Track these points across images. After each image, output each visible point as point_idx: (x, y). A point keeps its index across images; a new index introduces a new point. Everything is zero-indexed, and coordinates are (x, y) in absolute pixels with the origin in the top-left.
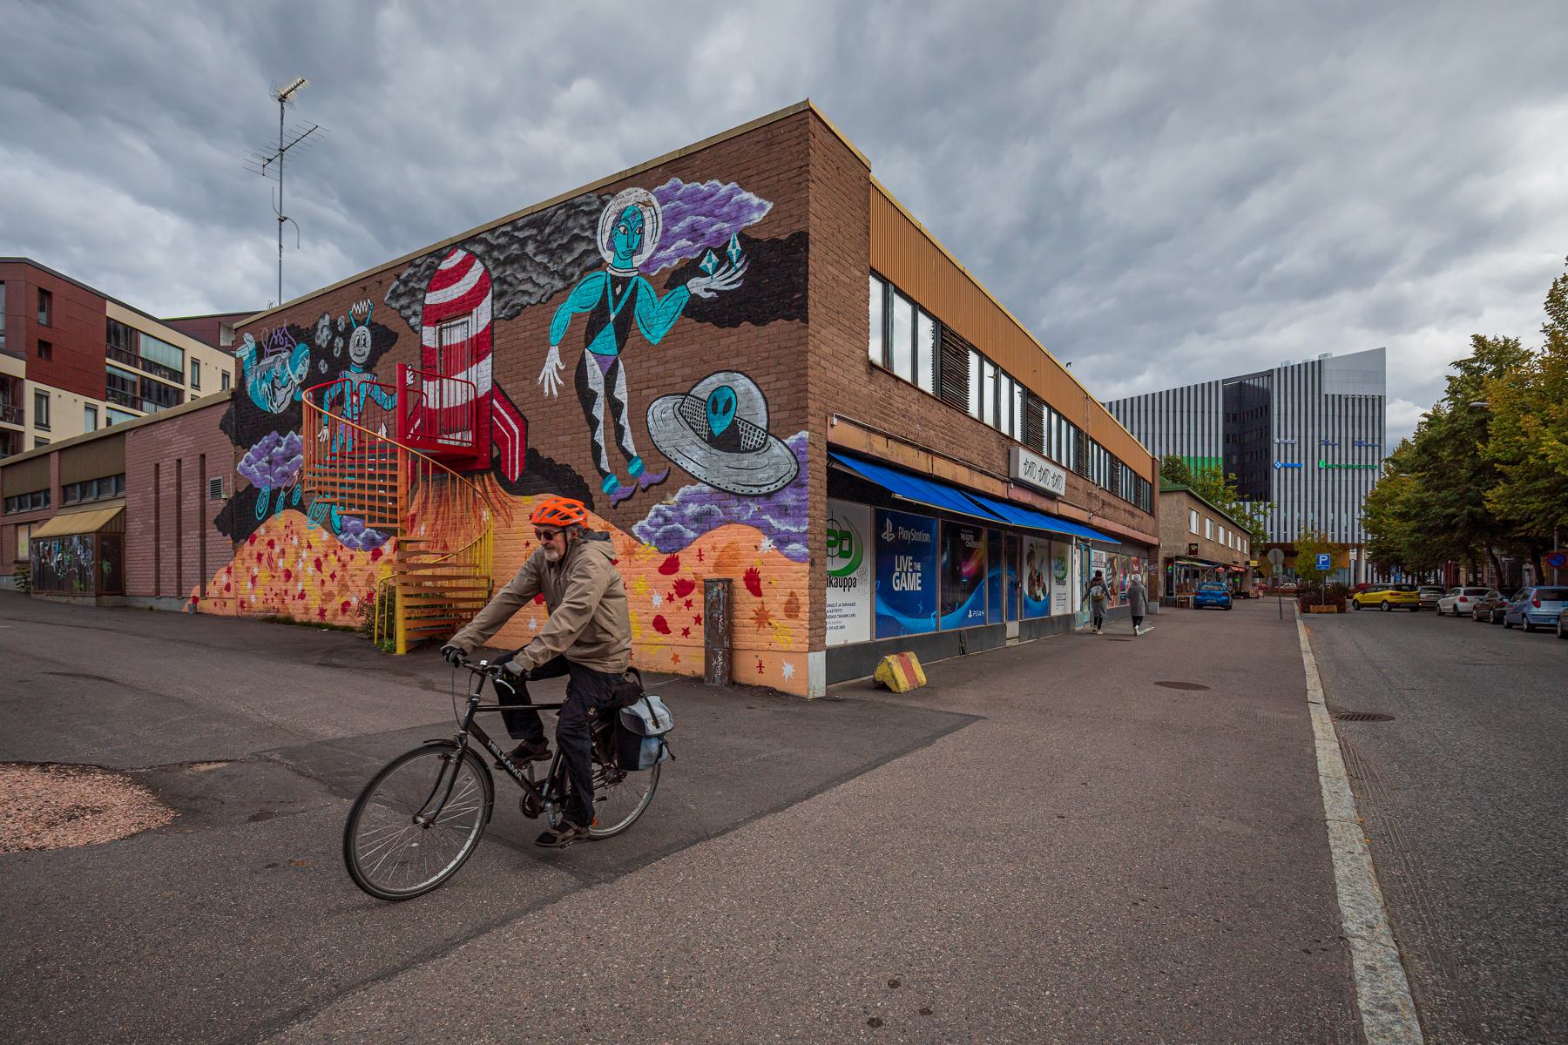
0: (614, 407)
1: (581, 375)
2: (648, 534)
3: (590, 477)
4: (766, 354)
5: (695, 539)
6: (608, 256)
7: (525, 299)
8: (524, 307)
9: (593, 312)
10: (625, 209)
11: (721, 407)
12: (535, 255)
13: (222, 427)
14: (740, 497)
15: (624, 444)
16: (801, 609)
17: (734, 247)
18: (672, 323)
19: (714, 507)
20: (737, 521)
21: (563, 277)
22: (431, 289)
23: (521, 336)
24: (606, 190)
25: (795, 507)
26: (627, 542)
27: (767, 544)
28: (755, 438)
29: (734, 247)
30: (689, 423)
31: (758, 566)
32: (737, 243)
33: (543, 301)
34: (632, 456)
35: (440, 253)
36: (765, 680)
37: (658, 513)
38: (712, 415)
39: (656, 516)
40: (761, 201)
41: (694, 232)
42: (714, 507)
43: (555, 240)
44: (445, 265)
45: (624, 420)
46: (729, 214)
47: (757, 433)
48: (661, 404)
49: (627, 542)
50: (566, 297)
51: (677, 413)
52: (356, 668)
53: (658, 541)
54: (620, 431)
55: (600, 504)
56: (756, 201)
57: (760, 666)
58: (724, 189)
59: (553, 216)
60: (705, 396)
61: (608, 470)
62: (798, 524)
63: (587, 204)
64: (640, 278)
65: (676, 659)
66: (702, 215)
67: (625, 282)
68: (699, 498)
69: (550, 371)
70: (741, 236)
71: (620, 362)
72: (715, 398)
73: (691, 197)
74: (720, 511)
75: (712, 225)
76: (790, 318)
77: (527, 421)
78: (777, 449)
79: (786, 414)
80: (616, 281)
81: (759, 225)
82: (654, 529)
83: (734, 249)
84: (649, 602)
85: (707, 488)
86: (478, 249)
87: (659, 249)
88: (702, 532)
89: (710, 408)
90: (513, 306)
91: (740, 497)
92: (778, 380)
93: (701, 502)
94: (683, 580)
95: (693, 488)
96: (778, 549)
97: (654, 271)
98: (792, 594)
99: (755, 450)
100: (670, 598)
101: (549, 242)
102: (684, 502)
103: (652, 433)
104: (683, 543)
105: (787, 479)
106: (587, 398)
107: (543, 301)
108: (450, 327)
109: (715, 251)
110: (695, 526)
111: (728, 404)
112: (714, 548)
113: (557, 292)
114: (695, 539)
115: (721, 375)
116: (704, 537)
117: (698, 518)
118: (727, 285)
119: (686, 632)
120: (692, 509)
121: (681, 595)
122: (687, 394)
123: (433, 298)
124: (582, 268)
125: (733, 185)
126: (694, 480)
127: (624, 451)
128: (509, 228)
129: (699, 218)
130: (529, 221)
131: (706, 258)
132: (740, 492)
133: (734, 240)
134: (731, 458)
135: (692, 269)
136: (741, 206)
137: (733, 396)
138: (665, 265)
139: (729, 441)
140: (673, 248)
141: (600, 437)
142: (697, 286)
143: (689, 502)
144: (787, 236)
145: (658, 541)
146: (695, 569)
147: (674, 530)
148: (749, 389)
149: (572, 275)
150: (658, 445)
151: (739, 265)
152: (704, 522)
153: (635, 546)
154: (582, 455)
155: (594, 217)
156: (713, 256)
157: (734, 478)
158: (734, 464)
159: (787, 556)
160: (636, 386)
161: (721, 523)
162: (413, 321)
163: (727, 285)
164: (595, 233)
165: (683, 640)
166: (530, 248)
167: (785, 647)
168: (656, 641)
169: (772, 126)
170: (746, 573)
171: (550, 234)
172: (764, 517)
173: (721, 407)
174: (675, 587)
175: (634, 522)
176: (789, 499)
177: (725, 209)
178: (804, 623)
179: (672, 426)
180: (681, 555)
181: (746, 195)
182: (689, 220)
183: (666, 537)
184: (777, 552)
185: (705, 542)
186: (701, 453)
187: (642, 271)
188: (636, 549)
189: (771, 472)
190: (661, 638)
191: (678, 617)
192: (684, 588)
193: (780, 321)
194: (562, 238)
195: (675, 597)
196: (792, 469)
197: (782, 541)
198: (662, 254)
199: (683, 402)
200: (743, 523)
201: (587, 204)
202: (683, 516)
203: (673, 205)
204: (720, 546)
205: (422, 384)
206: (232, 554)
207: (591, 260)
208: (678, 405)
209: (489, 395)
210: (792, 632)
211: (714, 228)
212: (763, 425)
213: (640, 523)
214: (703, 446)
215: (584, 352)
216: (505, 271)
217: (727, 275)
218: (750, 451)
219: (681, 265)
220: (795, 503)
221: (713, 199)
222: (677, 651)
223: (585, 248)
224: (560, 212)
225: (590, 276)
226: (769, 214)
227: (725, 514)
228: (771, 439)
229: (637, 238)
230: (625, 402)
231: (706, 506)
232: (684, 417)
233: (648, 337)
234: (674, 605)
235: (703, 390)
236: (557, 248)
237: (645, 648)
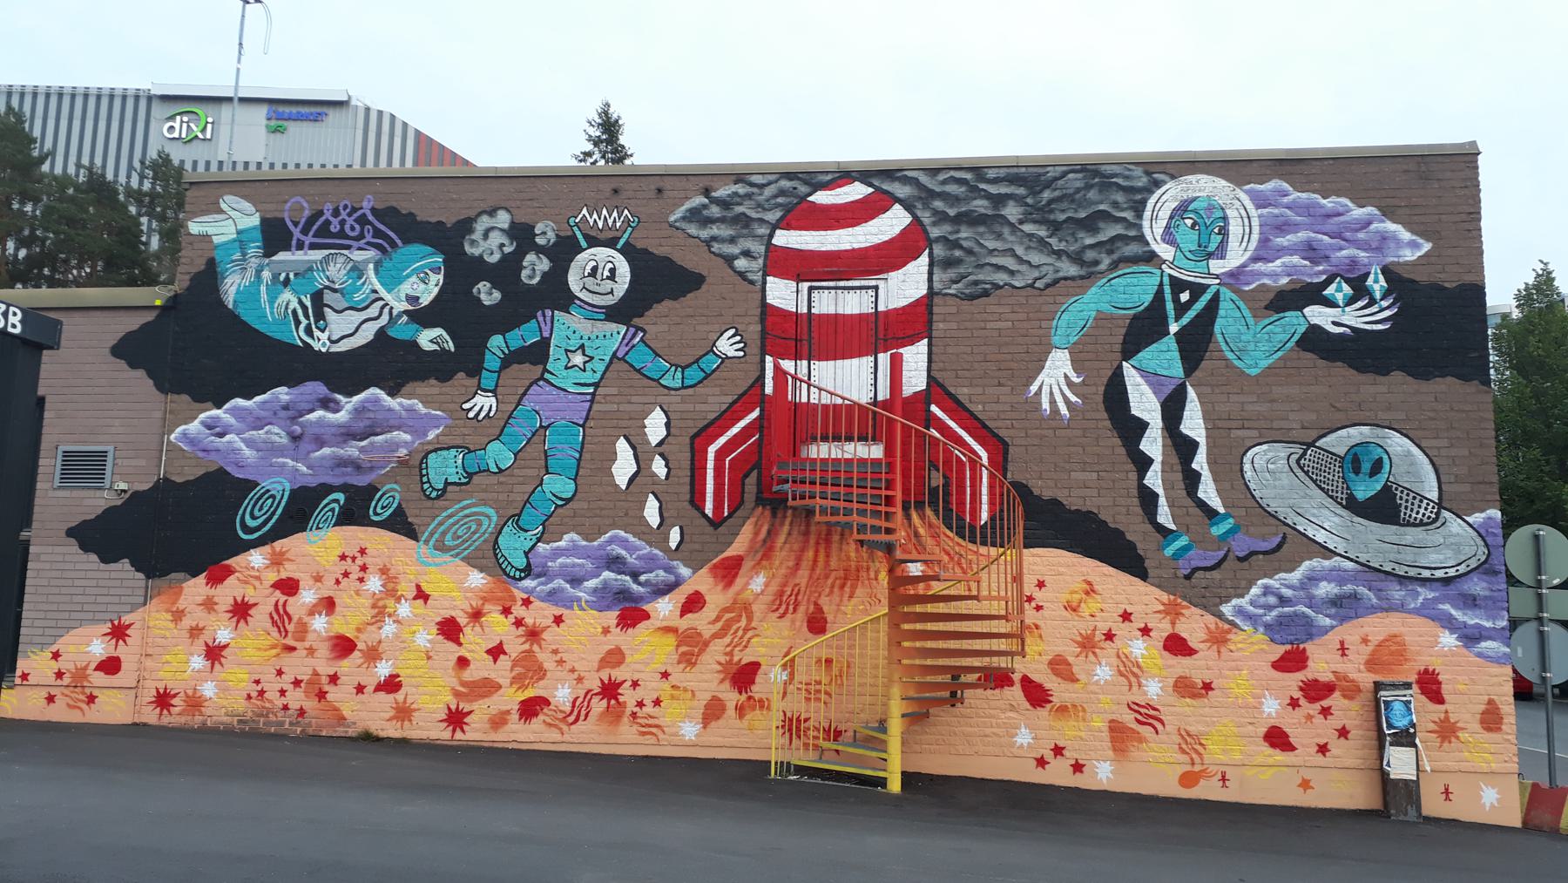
0: (1182, 448)
1: (1116, 395)
2: (1249, 617)
3: (1136, 530)
4: (1432, 414)
5: (1333, 627)
6: (1165, 251)
7: (1001, 278)
8: (997, 287)
9: (1135, 318)
10: (1194, 199)
11: (1366, 467)
12: (1021, 222)
13: (1475, 142)
14: (1403, 580)
15: (1201, 494)
16: (1505, 721)
17: (1376, 281)
18: (1280, 354)
19: (1362, 590)
20: (1401, 608)
21: (1077, 258)
22: (786, 224)
23: (991, 325)
24: (1160, 168)
25: (1486, 598)
26: (1212, 627)
27: (1449, 640)
28: (1422, 511)
29: (1376, 281)
30: (1315, 482)
31: (1436, 664)
32: (1381, 277)
33: (1037, 285)
34: (1215, 513)
35: (814, 178)
36: (1457, 810)
37: (1267, 591)
38: (1352, 475)
39: (1265, 594)
40: (1414, 238)
41: (1311, 252)
42: (1362, 590)
43: (1063, 211)
44: (822, 198)
45: (1200, 462)
46: (1366, 242)
47: (1424, 505)
48: (1269, 450)
49: (1212, 627)
50: (1084, 290)
51: (1294, 466)
52: (1345, 571)
53: (1268, 627)
54: (1192, 479)
55: (1157, 572)
56: (1406, 235)
57: (1447, 792)
58: (1358, 212)
59: (1056, 179)
60: (1341, 451)
61: (1173, 527)
62: (1494, 618)
63: (1127, 178)
64: (1223, 290)
65: (1305, 785)
66: (1324, 234)
67: (1197, 290)
68: (1339, 577)
69: (1053, 381)
70: (1386, 271)
71: (1190, 389)
72: (1355, 454)
73: (1308, 209)
74: (1371, 595)
75: (1341, 249)
76: (1465, 378)
77: (1006, 444)
78: (1455, 525)
79: (1467, 487)
80: (1178, 285)
81: (1406, 264)
82: (1261, 611)
83: (1377, 284)
84: (1258, 707)
85: (1350, 565)
86: (901, 191)
87: (1255, 259)
88: (1343, 619)
89: (1348, 466)
90: (976, 283)
91: (1403, 580)
92: (1452, 446)
93: (1341, 582)
94: (1316, 681)
95: (1327, 563)
96: (1466, 646)
97: (1248, 284)
98: (1491, 702)
99: (1421, 524)
100: (1294, 703)
101: (1051, 211)
102: (1312, 579)
103: (1252, 486)
104: (1311, 631)
105: (1473, 564)
106: (1133, 429)
107: (1037, 285)
108: (1249, 217)
109: (1347, 281)
110: (1333, 611)
111: (1377, 467)
112: (1365, 641)
113: (1066, 279)
114: (1333, 627)
115: (1365, 429)
116: (1346, 625)
117: (1336, 602)
118: (1051, 393)
119: (1323, 749)
120: (1325, 589)
121: (1312, 699)
122: (1311, 444)
123: (783, 238)
124: (1115, 256)
125: (1370, 210)
126: (1328, 552)
127: (1202, 505)
128: (968, 176)
129: (1320, 236)
130: (1008, 174)
131: (1334, 286)
132: (1402, 573)
133: (1376, 273)
134: (1389, 531)
135: (1313, 294)
136: (1384, 238)
137: (1385, 457)
138: (1266, 281)
139: (1384, 508)
140: (1278, 262)
141: (1154, 479)
142: (1318, 315)
143: (1320, 580)
144: (1454, 285)
145: (1268, 627)
146: (1335, 667)
147: (1296, 614)
148: (1409, 451)
149: (1097, 263)
150: (1263, 503)
151: (1385, 304)
152: (1345, 607)
153: (1229, 631)
154: (1122, 501)
155: (1138, 197)
156: (1345, 286)
157: (1392, 556)
158: (1394, 539)
159: (1480, 655)
160: (1220, 423)
161: (1374, 610)
162: (741, 264)
163: (1051, 393)
164: (1140, 216)
165: (1320, 759)
166: (1012, 212)
167: (1484, 767)
168: (1270, 761)
169: (1428, 159)
170: (1419, 673)
171: (1051, 202)
172: (1441, 606)
173: (1366, 467)
174: (1301, 689)
175: (1228, 599)
176: (1478, 586)
177: (1361, 235)
178: (1510, 737)
179: (1285, 482)
180: (1310, 648)
181: (1391, 226)
182: (1302, 235)
183: (1282, 624)
184: (1465, 651)
185: (1351, 632)
186: (1336, 519)
187: (1227, 280)
188: (1229, 636)
189: (1449, 553)
190: (1279, 756)
191: (1305, 728)
192: (1316, 691)
193: (1449, 379)
194: (1076, 211)
195: (1303, 702)
196: (1480, 552)
197: (1471, 637)
198: (1259, 266)
199: (1304, 454)
200: (1410, 612)
201: (1127, 178)
202: (1311, 597)
203: (1276, 211)
204: (1375, 639)
205: (763, 362)
206: (141, 600)
207: (1132, 249)
208: (1297, 456)
209: (923, 398)
210: (1492, 748)
211: (1344, 253)
212: (1434, 495)
213: (1235, 602)
214: (1338, 511)
215: (1120, 367)
216: (958, 232)
217: (1367, 311)
218: (1414, 525)
219: (1293, 286)
220: (1487, 593)
221: (1341, 219)
222: (1308, 774)
223: (1122, 231)
224: (1071, 176)
225: (1121, 272)
226: (1427, 255)
227: (1379, 598)
228: (1445, 514)
229: (1217, 239)
230: (1202, 441)
231: (1349, 588)
232: (1307, 473)
233: (1237, 363)
234: (1299, 714)
235: (1340, 442)
236: (1065, 221)
237: (1250, 772)
